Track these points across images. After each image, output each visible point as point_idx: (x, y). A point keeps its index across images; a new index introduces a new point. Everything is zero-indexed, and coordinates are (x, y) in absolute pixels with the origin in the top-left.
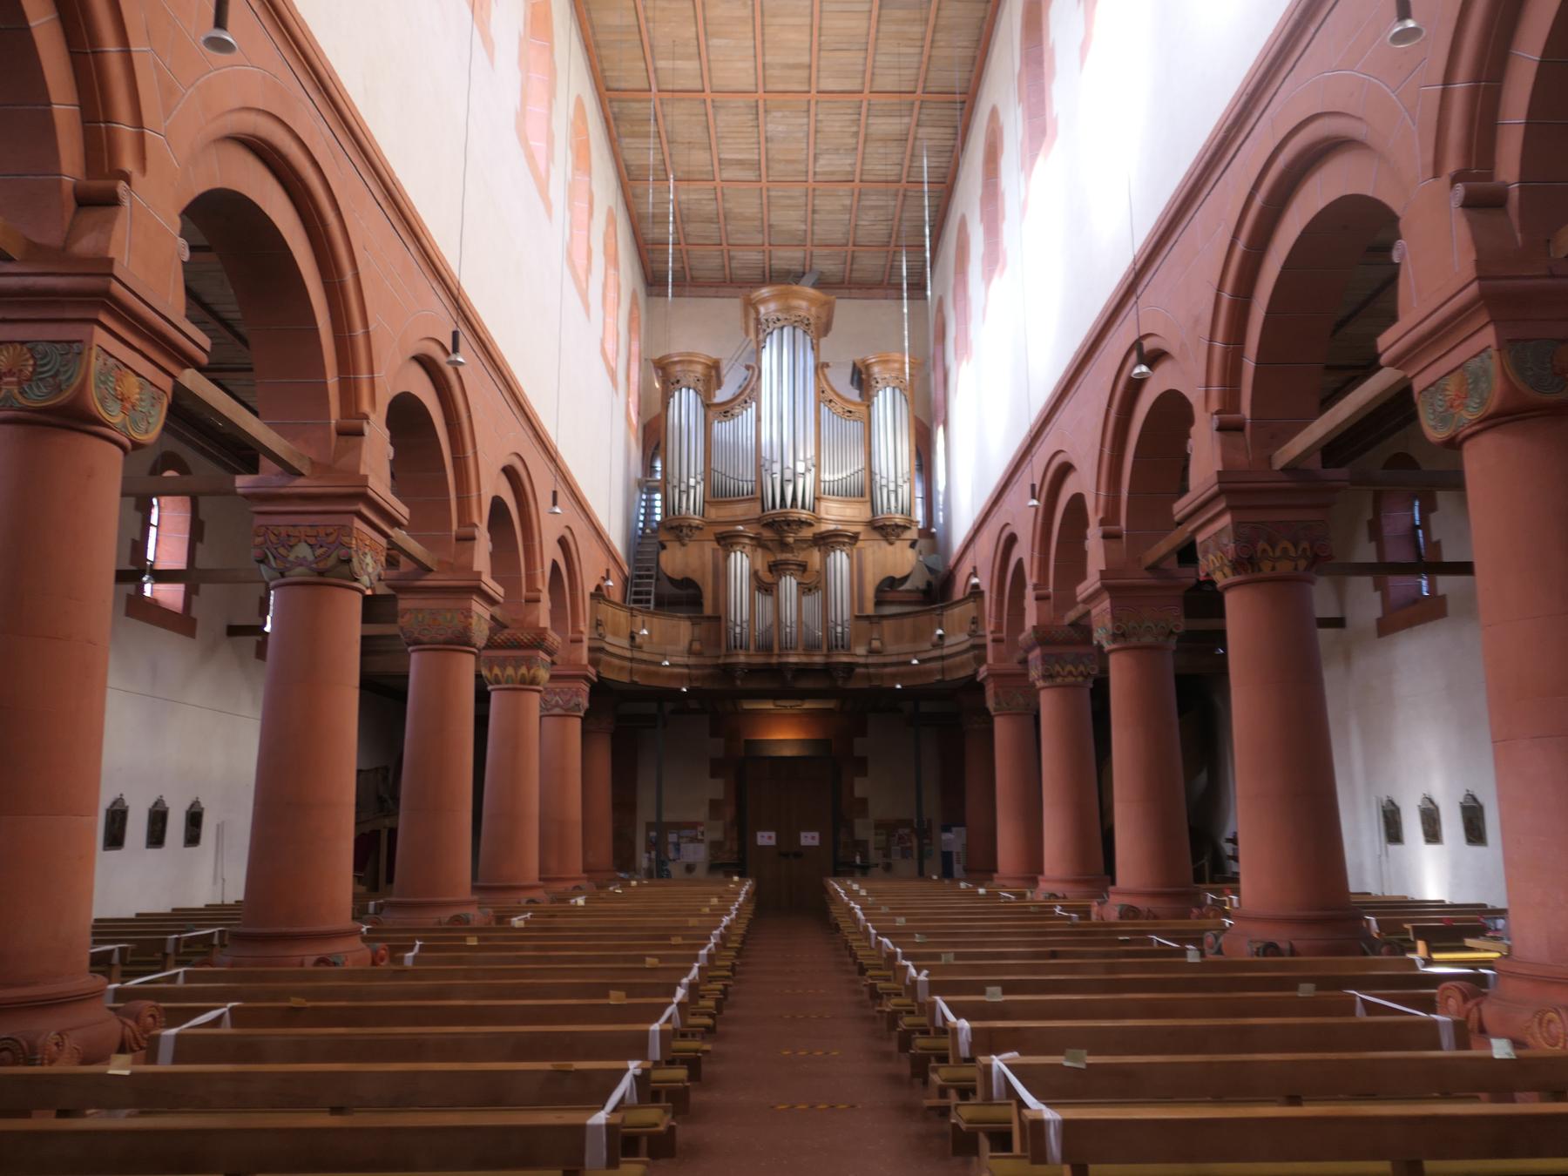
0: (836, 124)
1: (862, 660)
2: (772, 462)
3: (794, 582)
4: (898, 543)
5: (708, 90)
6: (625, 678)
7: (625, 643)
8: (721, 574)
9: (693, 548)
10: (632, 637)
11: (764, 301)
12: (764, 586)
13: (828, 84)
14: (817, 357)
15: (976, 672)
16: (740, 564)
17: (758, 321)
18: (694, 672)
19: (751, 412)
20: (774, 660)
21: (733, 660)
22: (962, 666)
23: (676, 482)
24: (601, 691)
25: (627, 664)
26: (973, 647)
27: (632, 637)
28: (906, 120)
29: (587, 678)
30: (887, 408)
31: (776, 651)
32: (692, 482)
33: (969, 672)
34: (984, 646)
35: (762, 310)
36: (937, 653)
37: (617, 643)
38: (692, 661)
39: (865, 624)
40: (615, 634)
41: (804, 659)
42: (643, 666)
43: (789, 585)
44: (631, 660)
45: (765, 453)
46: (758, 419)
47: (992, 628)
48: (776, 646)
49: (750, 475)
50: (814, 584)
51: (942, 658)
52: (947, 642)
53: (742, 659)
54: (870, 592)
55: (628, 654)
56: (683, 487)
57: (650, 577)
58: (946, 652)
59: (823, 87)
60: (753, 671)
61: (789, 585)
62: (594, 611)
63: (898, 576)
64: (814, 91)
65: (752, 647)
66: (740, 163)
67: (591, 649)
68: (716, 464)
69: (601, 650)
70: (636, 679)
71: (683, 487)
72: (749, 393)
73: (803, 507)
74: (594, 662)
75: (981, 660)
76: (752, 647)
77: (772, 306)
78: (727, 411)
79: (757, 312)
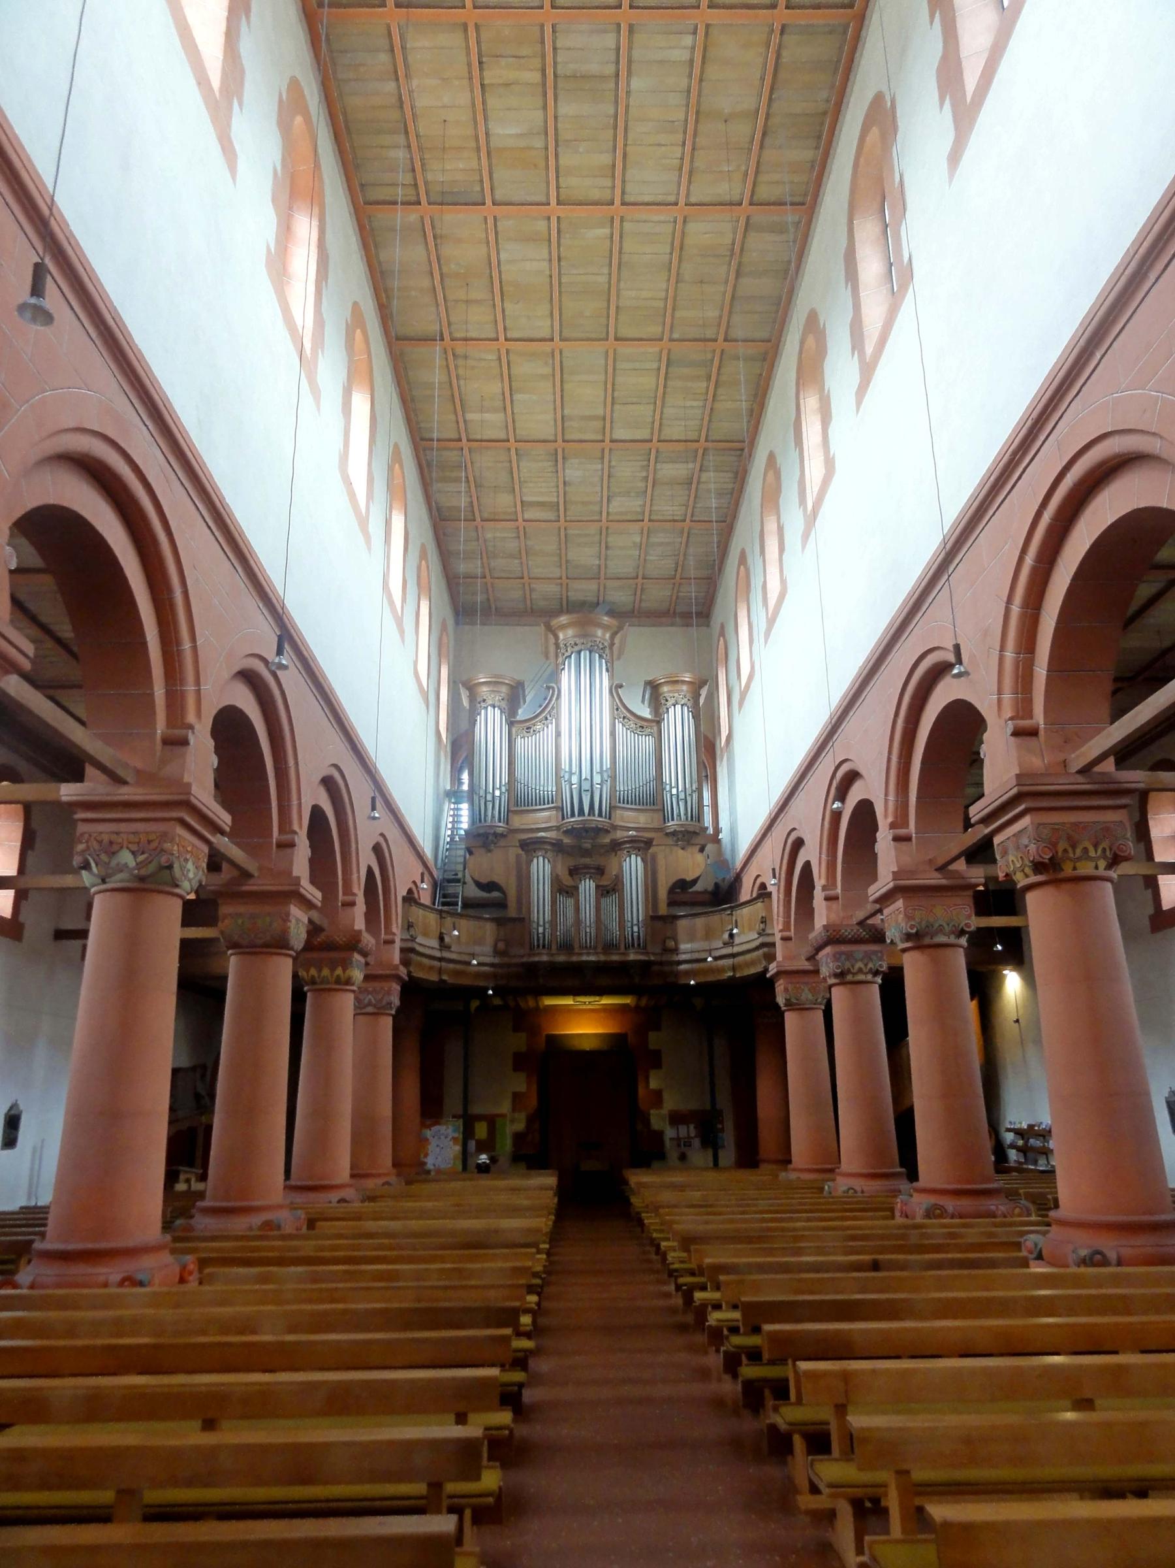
0: (627, 470)
1: (658, 958)
2: (571, 774)
3: (593, 885)
4: (690, 849)
5: (512, 440)
6: (434, 977)
7: (435, 943)
8: (524, 879)
10: (441, 939)
11: (563, 627)
12: (564, 890)
13: (620, 434)
14: (611, 678)
15: (766, 970)
16: (542, 869)
18: (500, 971)
20: (575, 959)
21: (536, 959)
22: (753, 963)
23: (482, 793)
24: (412, 989)
25: (436, 964)
26: (763, 945)
27: (441, 939)
28: (691, 466)
29: (397, 978)
30: (678, 723)
31: (576, 951)
32: (497, 793)
33: (759, 969)
34: (773, 945)
35: (561, 636)
37: (428, 943)
38: (496, 960)
39: (659, 924)
40: (426, 934)
41: (602, 958)
42: (451, 966)
43: (587, 887)
44: (440, 959)
45: (565, 765)
46: (558, 734)
47: (781, 927)
48: (576, 946)
49: (551, 788)
50: (611, 889)
51: (733, 956)
52: (737, 940)
53: (545, 958)
54: (663, 894)
55: (438, 954)
56: (489, 797)
57: (458, 881)
58: (736, 949)
59: (615, 437)
60: (554, 969)
61: (587, 887)
62: (405, 916)
64: (607, 439)
65: (554, 947)
66: (541, 504)
67: (402, 950)
68: (519, 774)
69: (412, 950)
70: (445, 977)
71: (489, 797)
72: (547, 710)
73: (600, 815)
74: (405, 962)
75: (771, 957)
76: (554, 947)
77: (570, 632)
78: (528, 726)
79: (556, 637)
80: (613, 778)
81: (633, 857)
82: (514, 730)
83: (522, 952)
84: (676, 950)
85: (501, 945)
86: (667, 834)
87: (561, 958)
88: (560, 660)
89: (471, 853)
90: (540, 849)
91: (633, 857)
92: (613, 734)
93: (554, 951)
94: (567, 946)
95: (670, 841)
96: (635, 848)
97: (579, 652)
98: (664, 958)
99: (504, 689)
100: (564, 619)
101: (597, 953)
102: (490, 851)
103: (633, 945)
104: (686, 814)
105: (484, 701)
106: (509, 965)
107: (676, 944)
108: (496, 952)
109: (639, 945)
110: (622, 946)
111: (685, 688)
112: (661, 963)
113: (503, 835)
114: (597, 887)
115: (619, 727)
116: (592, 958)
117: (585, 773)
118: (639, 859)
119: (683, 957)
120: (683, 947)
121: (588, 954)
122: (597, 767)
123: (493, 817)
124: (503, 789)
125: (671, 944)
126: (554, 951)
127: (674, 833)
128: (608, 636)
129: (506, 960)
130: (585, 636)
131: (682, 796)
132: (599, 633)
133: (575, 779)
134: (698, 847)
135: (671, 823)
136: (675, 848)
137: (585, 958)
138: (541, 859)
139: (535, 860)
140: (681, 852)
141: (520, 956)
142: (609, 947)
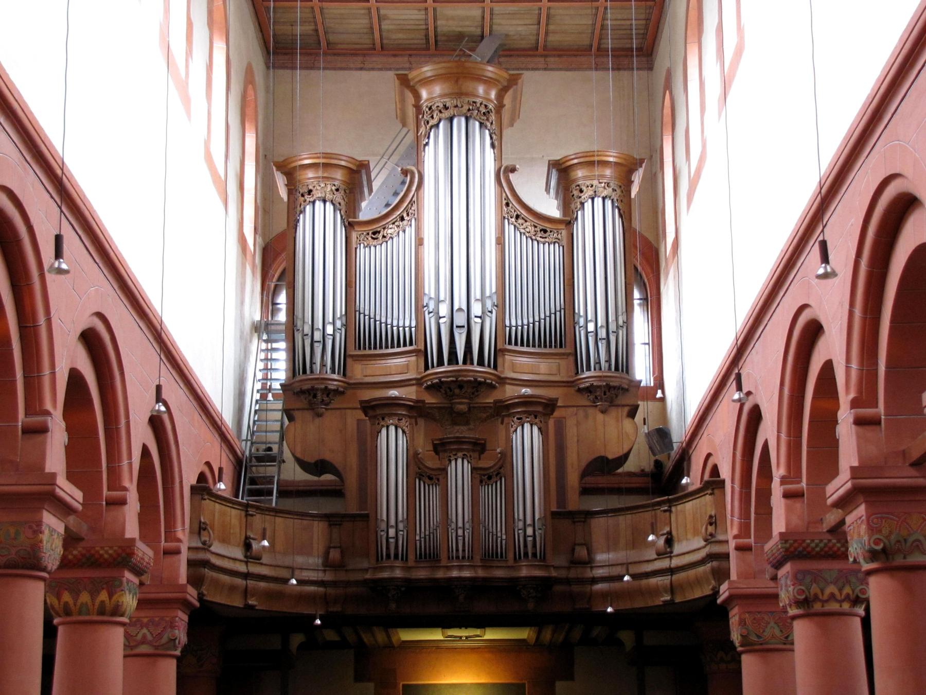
1: (563, 574)
4: (614, 412)
9: (331, 419)
16: (393, 444)
17: (418, 107)
18: (330, 591)
19: (411, 231)
20: (440, 574)
21: (386, 575)
23: (307, 330)
31: (444, 562)
36: (664, 564)
38: (328, 577)
41: (481, 573)
46: (420, 242)
48: (444, 556)
53: (398, 573)
56: (318, 336)
63: (611, 456)
65: (411, 557)
71: (318, 336)
73: (481, 363)
76: (411, 557)
78: (375, 230)
79: (417, 97)
80: (501, 306)
81: (527, 427)
82: (354, 235)
83: (365, 565)
84: (589, 562)
85: (335, 555)
86: (580, 390)
87: (422, 574)
88: (422, 130)
89: (291, 418)
90: (391, 415)
91: (527, 427)
92: (500, 242)
93: (411, 563)
94: (430, 557)
95: (584, 400)
96: (529, 413)
97: (451, 120)
98: (573, 574)
99: (339, 175)
100: (428, 70)
101: (474, 567)
102: (319, 415)
103: (526, 554)
104: (608, 361)
105: (310, 192)
106: (348, 584)
107: (590, 552)
108: (328, 565)
109: (534, 555)
110: (511, 555)
111: (608, 172)
112: (567, 581)
113: (337, 392)
114: (474, 469)
115: (509, 230)
116: (466, 574)
117: (460, 301)
118: (535, 429)
119: (599, 572)
120: (601, 557)
121: (461, 568)
122: (476, 292)
123: (323, 365)
124: (338, 324)
125: (582, 552)
126: (411, 563)
127: (589, 390)
128: (493, 95)
129: (342, 576)
130: (460, 94)
131: (602, 333)
132: (481, 90)
133: (444, 310)
134: (626, 409)
135: (587, 374)
136: (591, 411)
137: (455, 574)
138: (392, 429)
139: (384, 431)
140: (600, 416)
141: (362, 569)
142: (490, 557)
